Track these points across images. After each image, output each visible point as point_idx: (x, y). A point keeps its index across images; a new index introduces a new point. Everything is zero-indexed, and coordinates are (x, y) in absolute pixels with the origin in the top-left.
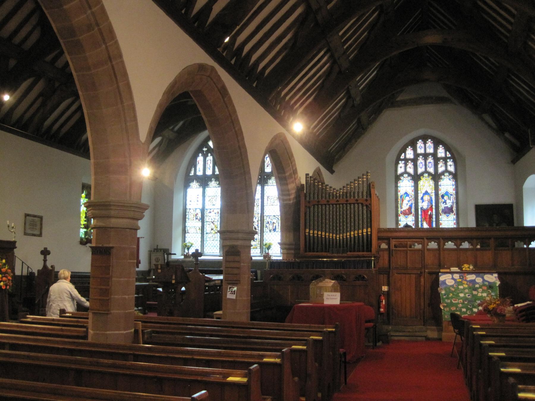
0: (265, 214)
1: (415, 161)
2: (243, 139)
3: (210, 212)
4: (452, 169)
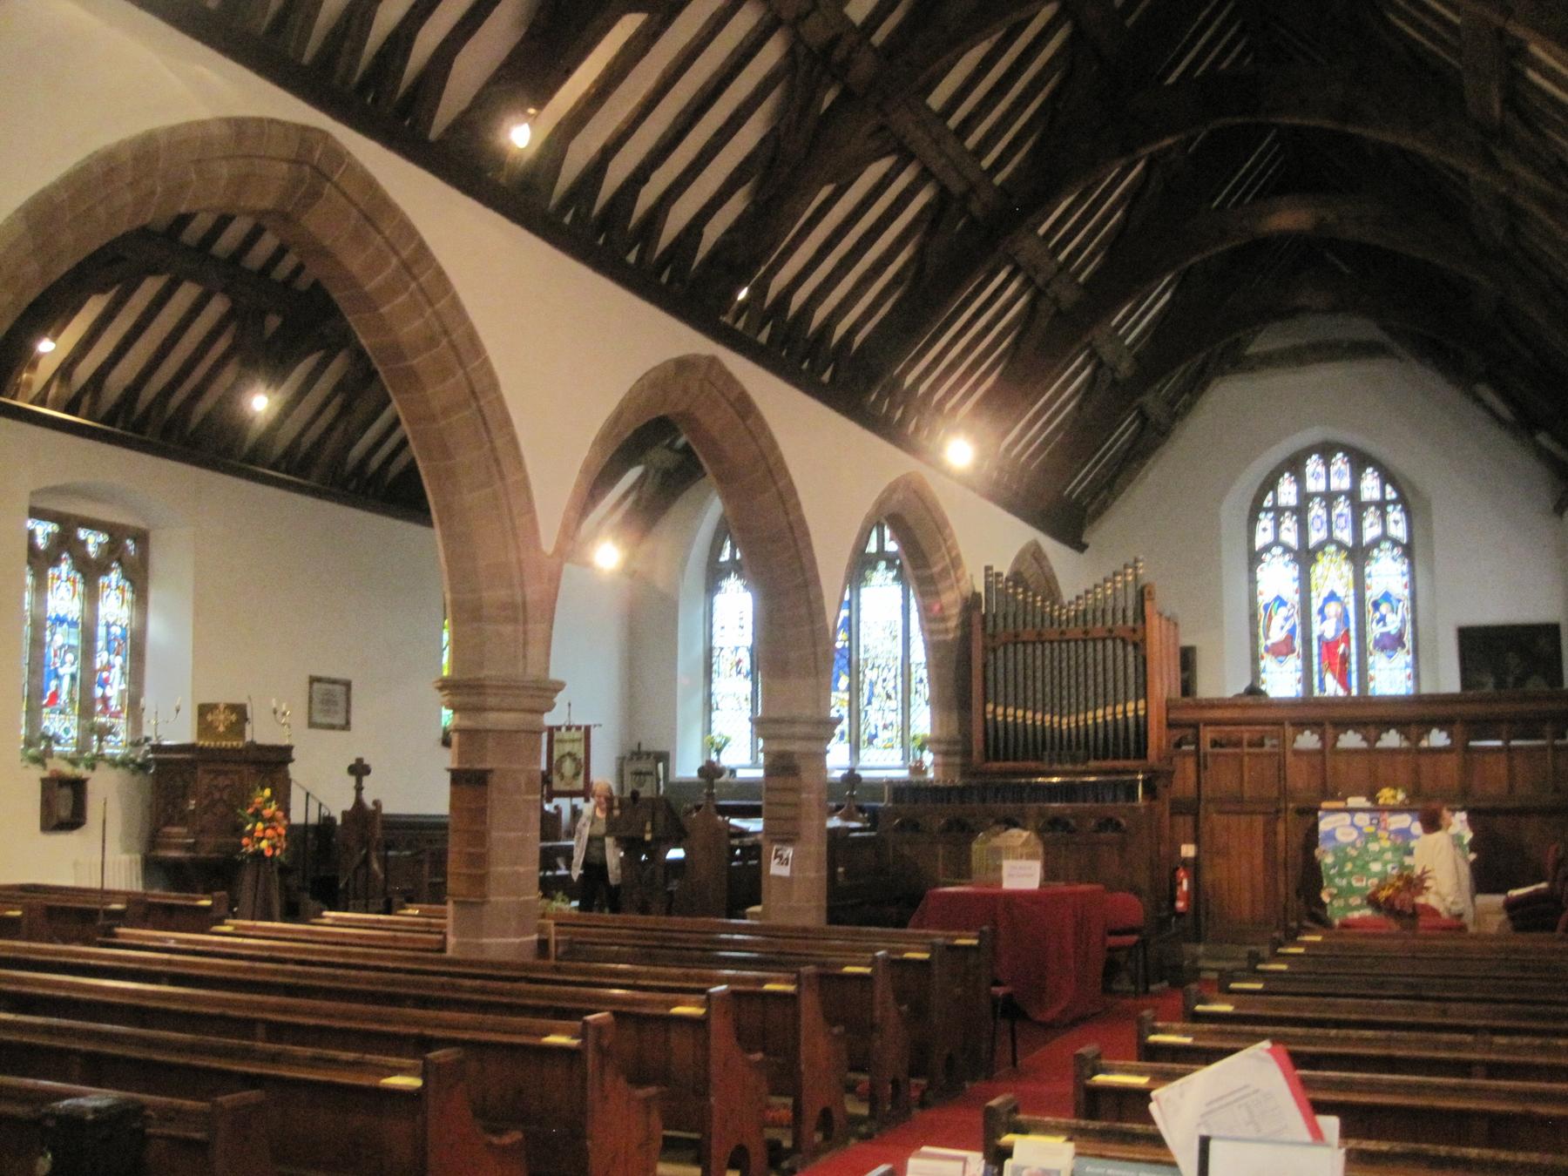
1: (1301, 511)
2: (798, 505)
4: (1399, 530)
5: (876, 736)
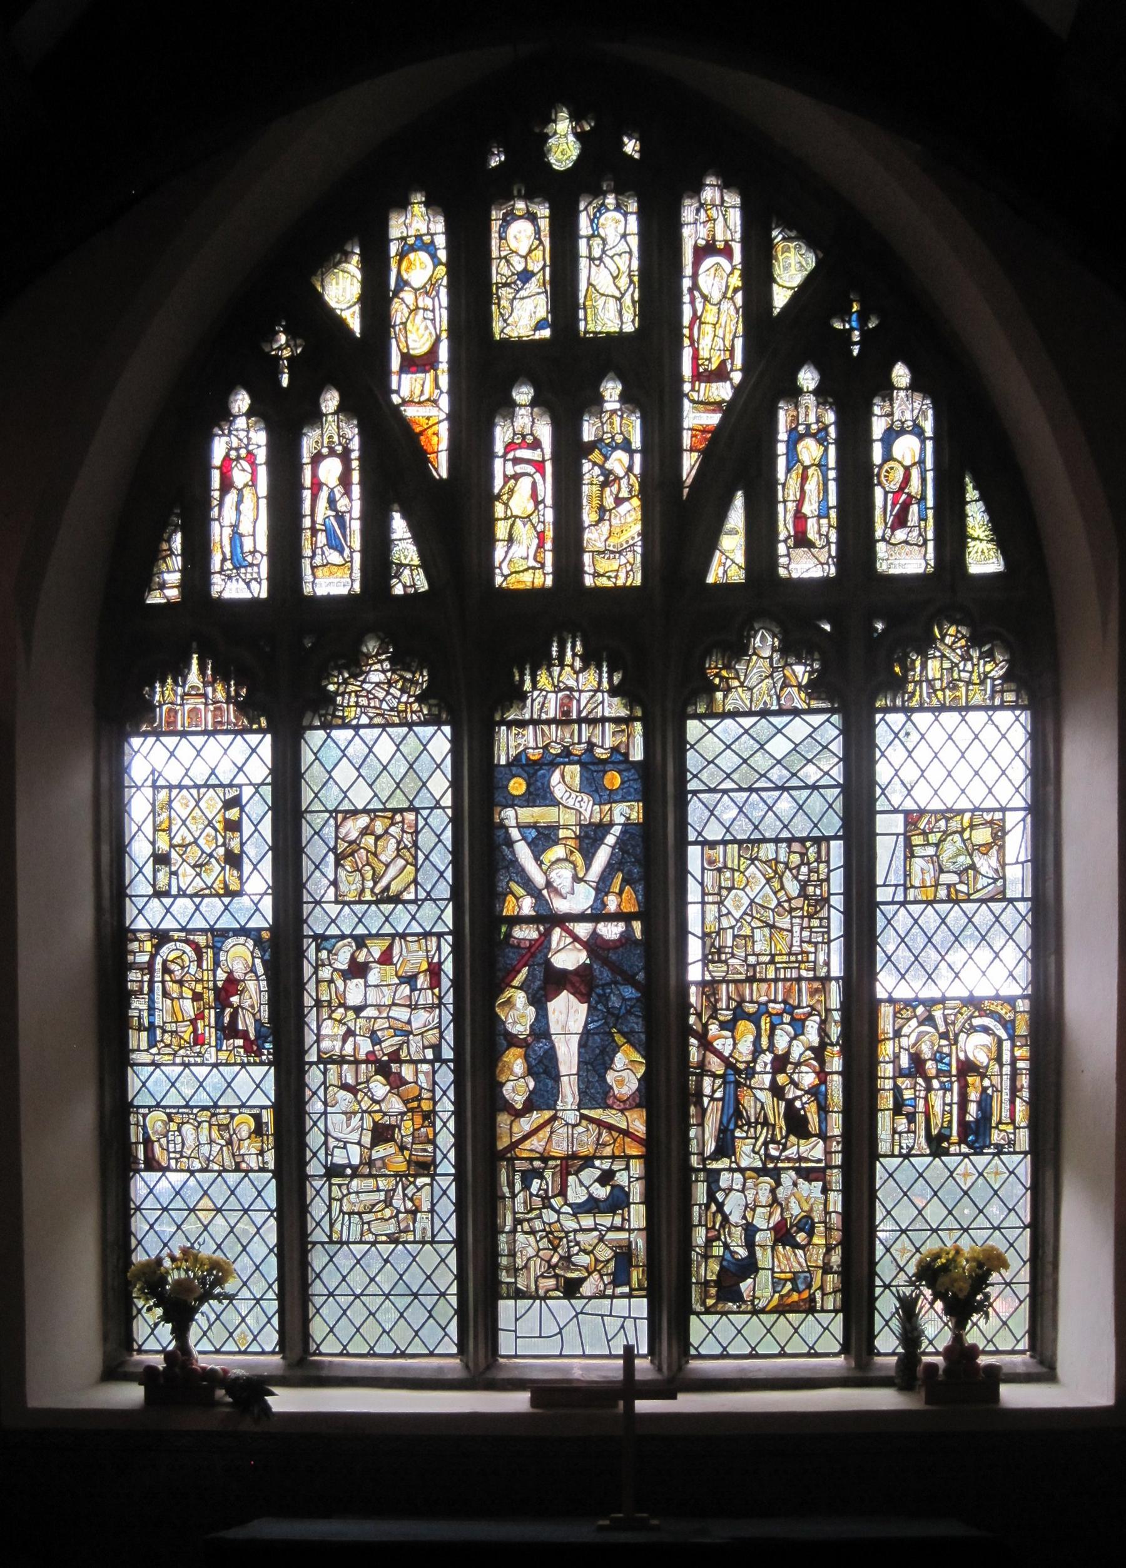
0: (886, 984)
3: (357, 970)
5: (750, 1267)
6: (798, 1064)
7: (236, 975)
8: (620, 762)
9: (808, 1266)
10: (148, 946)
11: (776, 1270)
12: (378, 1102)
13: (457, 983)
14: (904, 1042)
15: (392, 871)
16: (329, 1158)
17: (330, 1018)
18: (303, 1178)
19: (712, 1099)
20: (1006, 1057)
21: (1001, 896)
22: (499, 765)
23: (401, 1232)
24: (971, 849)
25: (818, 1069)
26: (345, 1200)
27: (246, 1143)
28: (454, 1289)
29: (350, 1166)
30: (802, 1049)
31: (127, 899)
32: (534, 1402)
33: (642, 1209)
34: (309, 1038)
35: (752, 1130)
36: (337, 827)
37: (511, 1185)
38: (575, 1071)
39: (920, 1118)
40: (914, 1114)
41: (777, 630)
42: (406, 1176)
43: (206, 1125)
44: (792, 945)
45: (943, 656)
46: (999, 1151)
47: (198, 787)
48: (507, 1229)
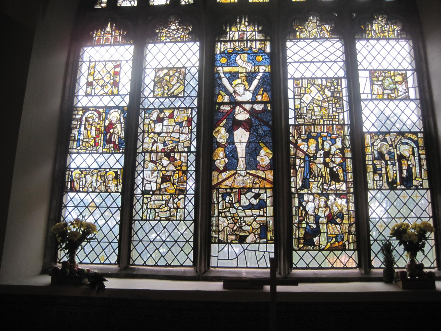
3: (160, 120)
5: (317, 232)
6: (334, 155)
7: (113, 122)
8: (262, 53)
9: (342, 232)
10: (81, 112)
11: (328, 233)
12: (165, 167)
13: (198, 125)
14: (375, 147)
15: (175, 87)
16: (144, 187)
17: (148, 136)
18: (133, 195)
19: (300, 167)
20: (416, 154)
21: (407, 98)
22: (217, 54)
23: (171, 216)
24: (395, 83)
25: (342, 156)
26: (149, 203)
27: (111, 182)
28: (192, 239)
29: (152, 190)
30: (335, 149)
31: (75, 98)
32: (225, 286)
33: (272, 208)
34: (139, 144)
35: (316, 179)
36: (156, 73)
37: (217, 198)
38: (244, 156)
39: (384, 175)
40: (382, 173)
41: (318, 15)
42: (175, 195)
43: (96, 175)
44: (329, 113)
45: (378, 23)
46: (417, 188)
47: (106, 61)
48: (215, 216)
